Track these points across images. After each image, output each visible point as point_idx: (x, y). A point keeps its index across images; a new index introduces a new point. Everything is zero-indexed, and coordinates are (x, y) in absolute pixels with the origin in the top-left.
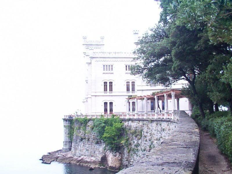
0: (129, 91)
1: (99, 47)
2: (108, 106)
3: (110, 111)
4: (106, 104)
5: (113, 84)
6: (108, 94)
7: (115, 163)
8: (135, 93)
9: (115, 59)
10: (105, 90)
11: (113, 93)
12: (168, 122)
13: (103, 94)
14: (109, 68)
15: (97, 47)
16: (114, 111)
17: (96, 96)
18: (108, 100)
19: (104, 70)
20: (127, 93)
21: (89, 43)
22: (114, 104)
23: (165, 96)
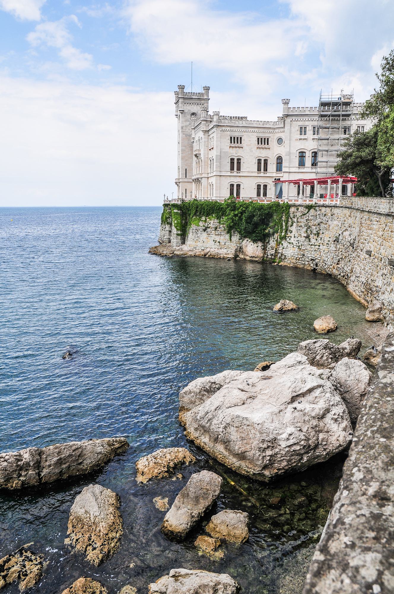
0: (260, 170)
1: (203, 102)
2: (235, 189)
3: (237, 195)
4: (232, 186)
5: (242, 161)
6: (235, 174)
7: (257, 253)
8: (268, 173)
9: (245, 129)
10: (232, 169)
11: (241, 173)
12: (331, 208)
13: (229, 174)
14: (236, 140)
15: (198, 102)
16: (241, 196)
17: (220, 176)
18: (235, 181)
19: (231, 143)
20: (258, 173)
21: (188, 96)
22: (241, 187)
23: (329, 181)
